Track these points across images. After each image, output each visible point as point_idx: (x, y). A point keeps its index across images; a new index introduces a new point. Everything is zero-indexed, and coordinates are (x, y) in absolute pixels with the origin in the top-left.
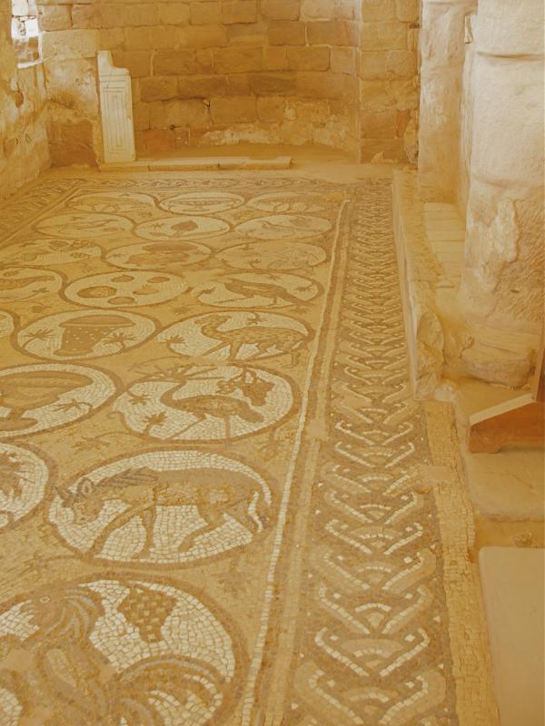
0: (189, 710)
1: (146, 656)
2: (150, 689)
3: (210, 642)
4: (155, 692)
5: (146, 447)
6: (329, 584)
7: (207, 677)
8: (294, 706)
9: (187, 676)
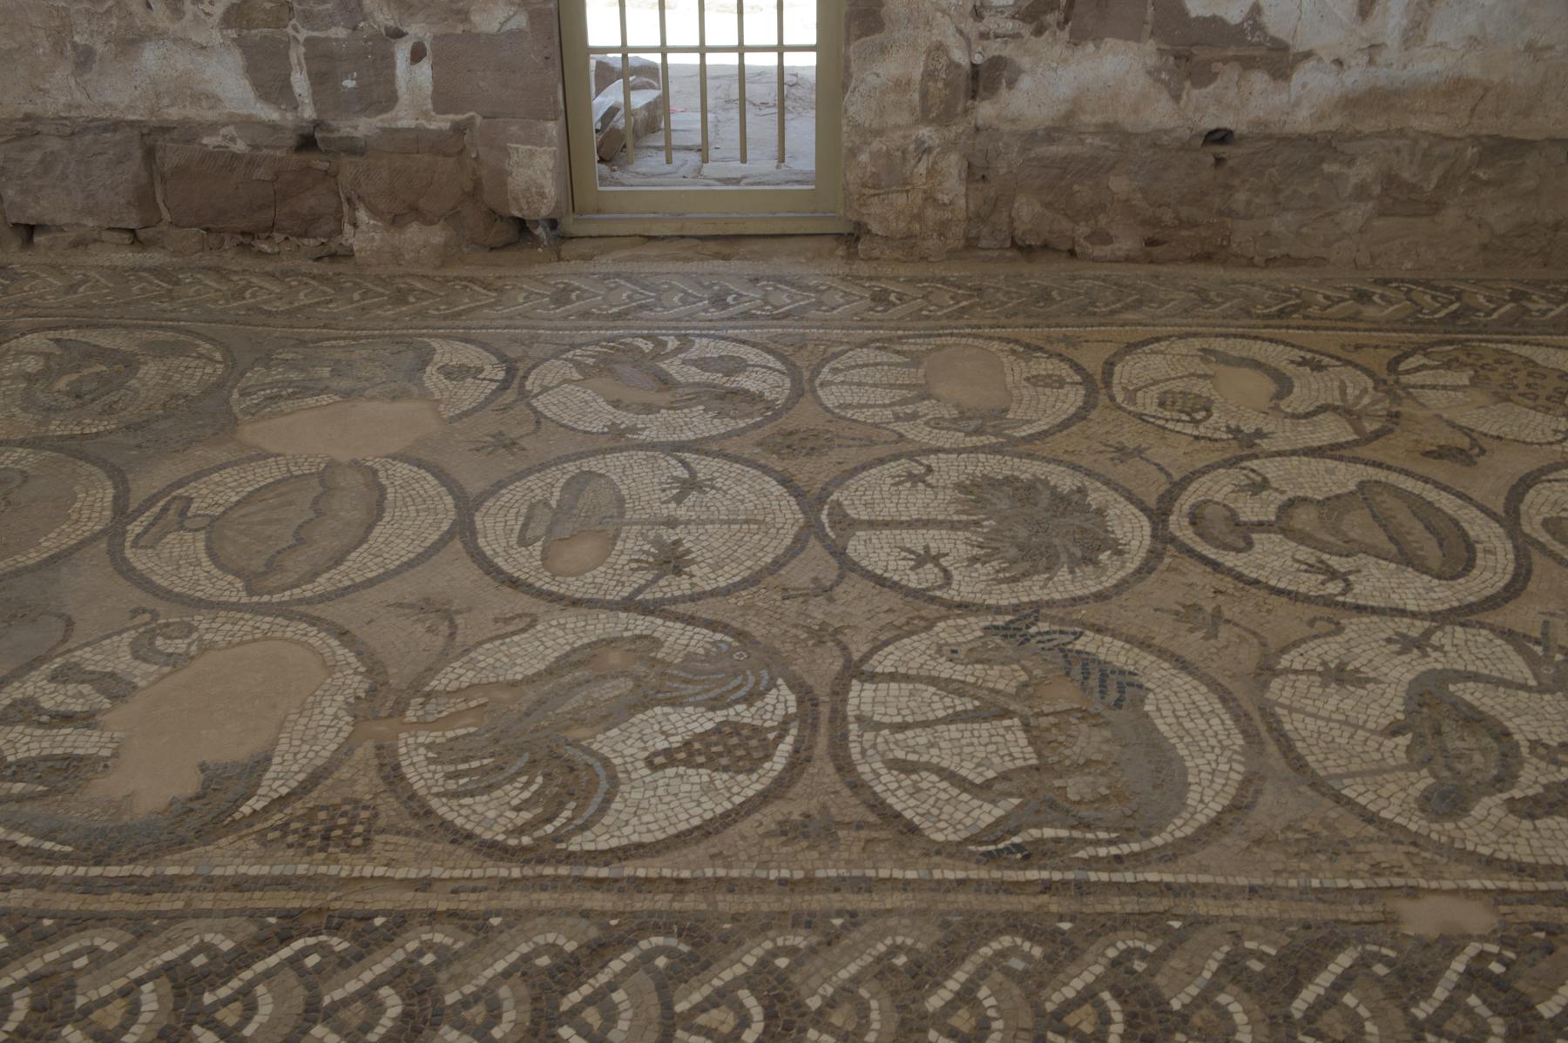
0: (501, 816)
1: (617, 761)
2: (547, 776)
3: (645, 819)
4: (540, 780)
5: (1225, 682)
6: (813, 950)
7: (563, 825)
8: (495, 921)
9: (573, 804)
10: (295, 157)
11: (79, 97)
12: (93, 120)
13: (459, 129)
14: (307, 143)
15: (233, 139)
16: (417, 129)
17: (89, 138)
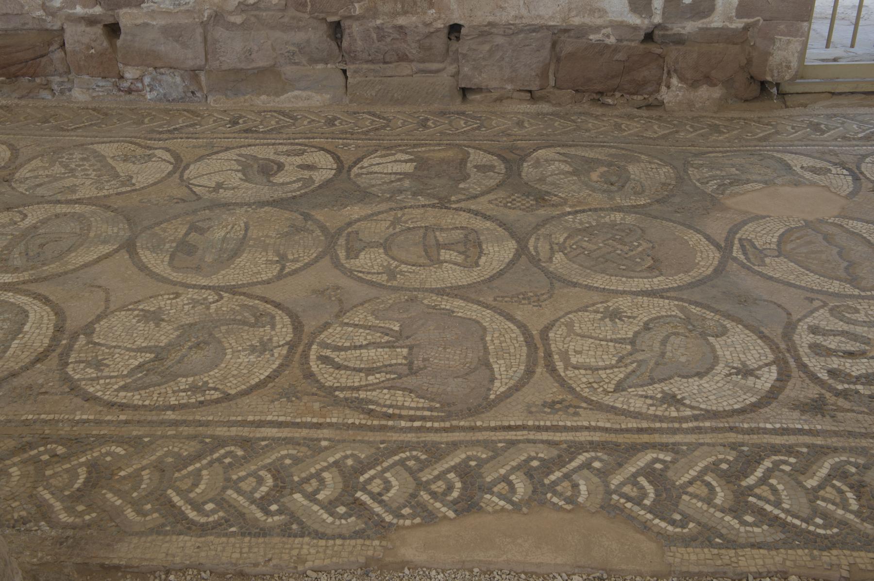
10: (642, 46)
11: (524, 12)
12: (529, 25)
13: (746, 28)
14: (649, 37)
15: (608, 36)
16: (722, 28)
17: (522, 36)
